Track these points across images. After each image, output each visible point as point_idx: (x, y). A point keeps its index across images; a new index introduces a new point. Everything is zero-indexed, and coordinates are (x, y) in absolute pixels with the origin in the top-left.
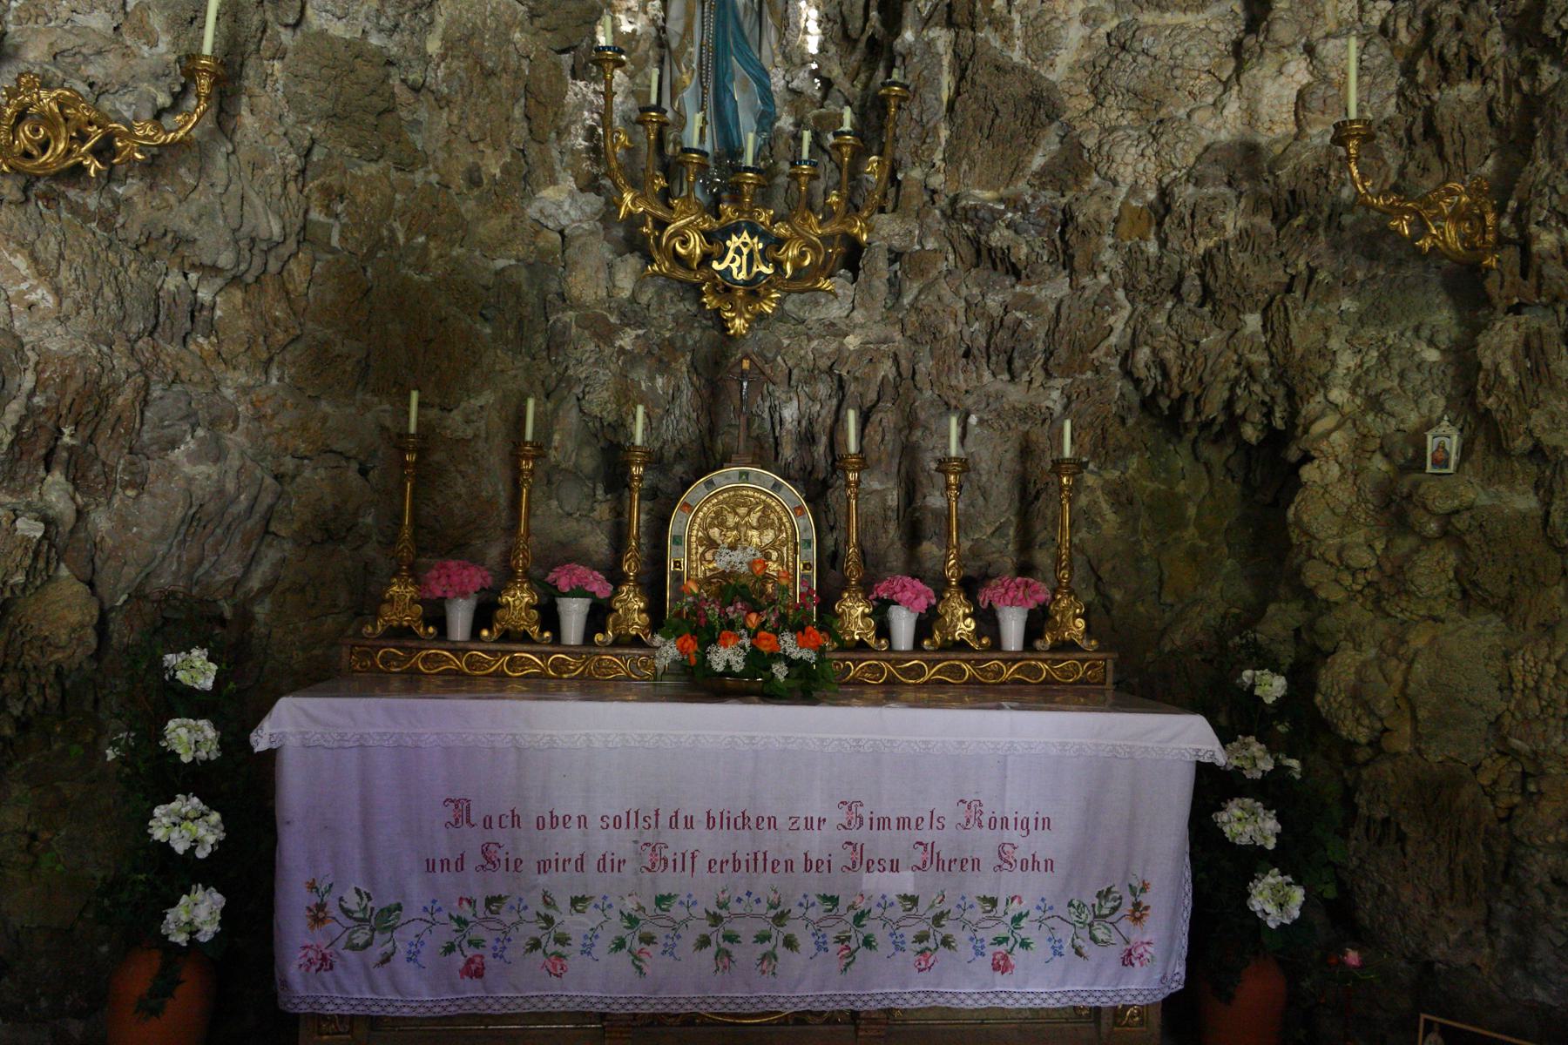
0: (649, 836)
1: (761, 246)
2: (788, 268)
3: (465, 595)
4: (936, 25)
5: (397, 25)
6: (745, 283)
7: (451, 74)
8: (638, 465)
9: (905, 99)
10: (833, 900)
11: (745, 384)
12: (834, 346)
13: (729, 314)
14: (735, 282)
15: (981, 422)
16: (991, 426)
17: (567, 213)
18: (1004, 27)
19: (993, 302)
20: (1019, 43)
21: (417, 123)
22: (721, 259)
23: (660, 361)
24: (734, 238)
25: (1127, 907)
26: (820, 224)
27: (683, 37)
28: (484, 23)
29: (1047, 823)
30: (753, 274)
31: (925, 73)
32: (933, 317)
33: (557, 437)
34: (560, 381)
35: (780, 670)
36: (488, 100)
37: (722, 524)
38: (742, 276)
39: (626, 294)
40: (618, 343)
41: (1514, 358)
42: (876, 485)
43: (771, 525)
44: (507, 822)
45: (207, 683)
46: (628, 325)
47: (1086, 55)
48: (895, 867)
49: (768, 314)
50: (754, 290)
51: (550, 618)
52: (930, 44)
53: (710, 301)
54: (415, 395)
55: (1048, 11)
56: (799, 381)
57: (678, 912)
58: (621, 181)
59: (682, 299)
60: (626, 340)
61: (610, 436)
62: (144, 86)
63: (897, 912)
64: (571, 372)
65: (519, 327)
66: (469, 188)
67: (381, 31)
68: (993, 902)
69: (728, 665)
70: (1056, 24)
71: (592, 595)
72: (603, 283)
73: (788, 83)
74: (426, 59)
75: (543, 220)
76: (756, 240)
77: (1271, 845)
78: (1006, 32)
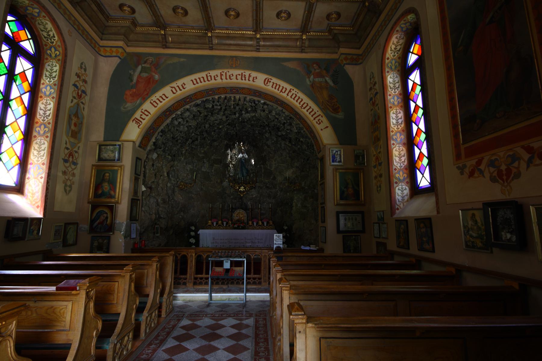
19: (268, 192)
35: (240, 227)
45: (194, 229)
50: (243, 192)
51: (223, 224)
53: (239, 193)
60: (232, 197)
74: (212, 172)
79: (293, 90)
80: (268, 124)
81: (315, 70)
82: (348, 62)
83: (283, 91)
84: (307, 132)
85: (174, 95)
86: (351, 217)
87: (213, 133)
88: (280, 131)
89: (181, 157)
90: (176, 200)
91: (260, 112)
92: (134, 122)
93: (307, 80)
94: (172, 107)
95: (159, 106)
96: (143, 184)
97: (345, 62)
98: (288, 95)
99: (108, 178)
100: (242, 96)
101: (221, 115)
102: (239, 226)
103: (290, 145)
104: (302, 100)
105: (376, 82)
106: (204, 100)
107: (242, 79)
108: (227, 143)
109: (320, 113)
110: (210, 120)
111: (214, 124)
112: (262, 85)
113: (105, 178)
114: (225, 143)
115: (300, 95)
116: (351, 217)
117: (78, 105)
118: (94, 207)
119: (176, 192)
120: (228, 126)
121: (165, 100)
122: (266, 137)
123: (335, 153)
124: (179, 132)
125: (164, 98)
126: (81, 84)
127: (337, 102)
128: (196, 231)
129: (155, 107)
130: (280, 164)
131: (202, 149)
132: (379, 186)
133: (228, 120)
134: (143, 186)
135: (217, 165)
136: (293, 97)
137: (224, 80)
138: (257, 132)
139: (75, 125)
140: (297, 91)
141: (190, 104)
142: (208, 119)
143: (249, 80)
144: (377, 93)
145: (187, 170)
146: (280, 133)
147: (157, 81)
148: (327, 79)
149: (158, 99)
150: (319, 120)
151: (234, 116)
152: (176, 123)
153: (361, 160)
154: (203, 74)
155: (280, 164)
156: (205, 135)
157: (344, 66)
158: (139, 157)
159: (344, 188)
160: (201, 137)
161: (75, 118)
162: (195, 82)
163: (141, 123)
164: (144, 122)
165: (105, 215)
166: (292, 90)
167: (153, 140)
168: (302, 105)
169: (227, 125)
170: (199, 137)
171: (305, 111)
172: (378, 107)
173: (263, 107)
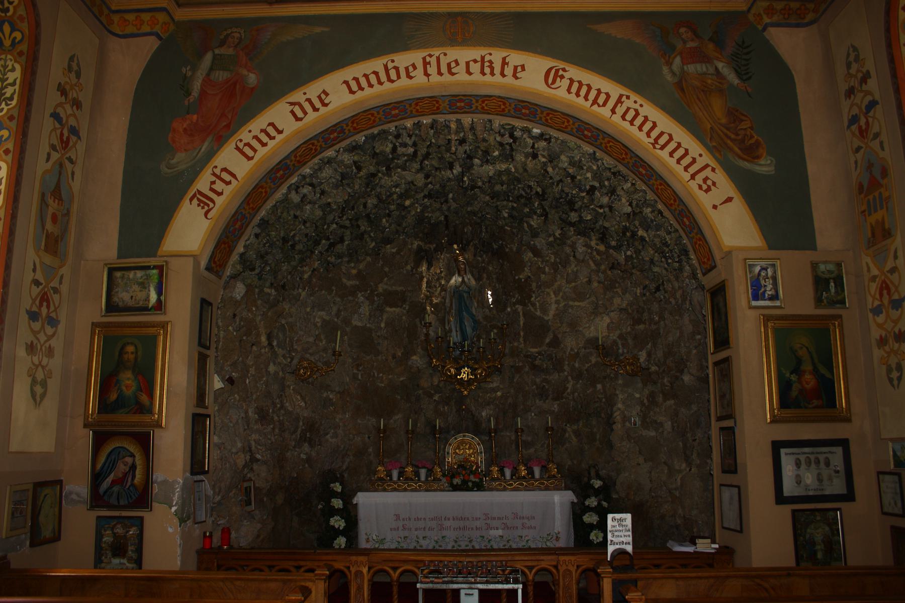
0: (440, 522)
3: (396, 469)
10: (483, 537)
15: (535, 415)
21: (379, 343)
22: (460, 375)
25: (555, 538)
29: (534, 518)
33: (419, 425)
35: (470, 484)
37: (459, 448)
39: (436, 383)
41: (647, 398)
42: (508, 434)
43: (472, 448)
44: (408, 519)
45: (339, 490)
47: (557, 312)
48: (497, 529)
51: (417, 474)
53: (458, 387)
57: (447, 540)
60: (436, 398)
62: (321, 353)
63: (498, 539)
68: (522, 537)
69: (457, 483)
70: (548, 305)
71: (427, 468)
77: (595, 523)
79: (628, 97)
80: (543, 191)
81: (685, 42)
82: (775, 18)
83: (601, 101)
84: (666, 213)
85: (299, 124)
86: (812, 457)
87: (384, 220)
88: (576, 211)
89: (300, 290)
90: (290, 409)
91: (523, 160)
92: (195, 201)
93: (665, 70)
94: (293, 158)
95: (258, 157)
96: (217, 372)
97: (767, 20)
98: (613, 111)
99: (132, 357)
100: (479, 118)
101: (413, 170)
102: (465, 482)
103: (602, 248)
104: (655, 125)
105: (868, 72)
106: (376, 132)
107: (483, 74)
108: (419, 247)
109: (707, 159)
110: (381, 187)
111: (392, 194)
112: (541, 87)
113: (126, 356)
114: (415, 246)
115: (649, 110)
116: (812, 457)
117: (61, 165)
118: (100, 440)
119: (289, 387)
120: (426, 200)
121: (274, 138)
122: (530, 226)
123: (759, 274)
124: (300, 222)
125: (273, 132)
126: (69, 112)
127: (752, 128)
128: (347, 496)
129: (250, 158)
130: (571, 303)
131: (352, 265)
132: (894, 366)
133: (431, 183)
134: (216, 378)
135: (394, 309)
136: (629, 117)
137: (435, 78)
138: (506, 215)
139: (54, 219)
140: (640, 101)
141: (337, 147)
142: (377, 184)
143: (503, 75)
144: (872, 104)
145: (315, 325)
146: (574, 217)
147: (253, 89)
148: (720, 65)
149: (256, 137)
150: (705, 180)
151: (448, 174)
152: (295, 198)
153: (833, 290)
154: (377, 64)
155: (571, 303)
156: (364, 226)
157: (764, 29)
158: (205, 297)
159: (791, 373)
160: (352, 233)
161: (54, 201)
162: (354, 87)
163: (211, 205)
164: (219, 200)
165: (129, 460)
166: (624, 98)
167: (240, 249)
168: (656, 140)
169: (425, 197)
170: (348, 232)
171: (664, 154)
172: (881, 143)
173: (533, 147)
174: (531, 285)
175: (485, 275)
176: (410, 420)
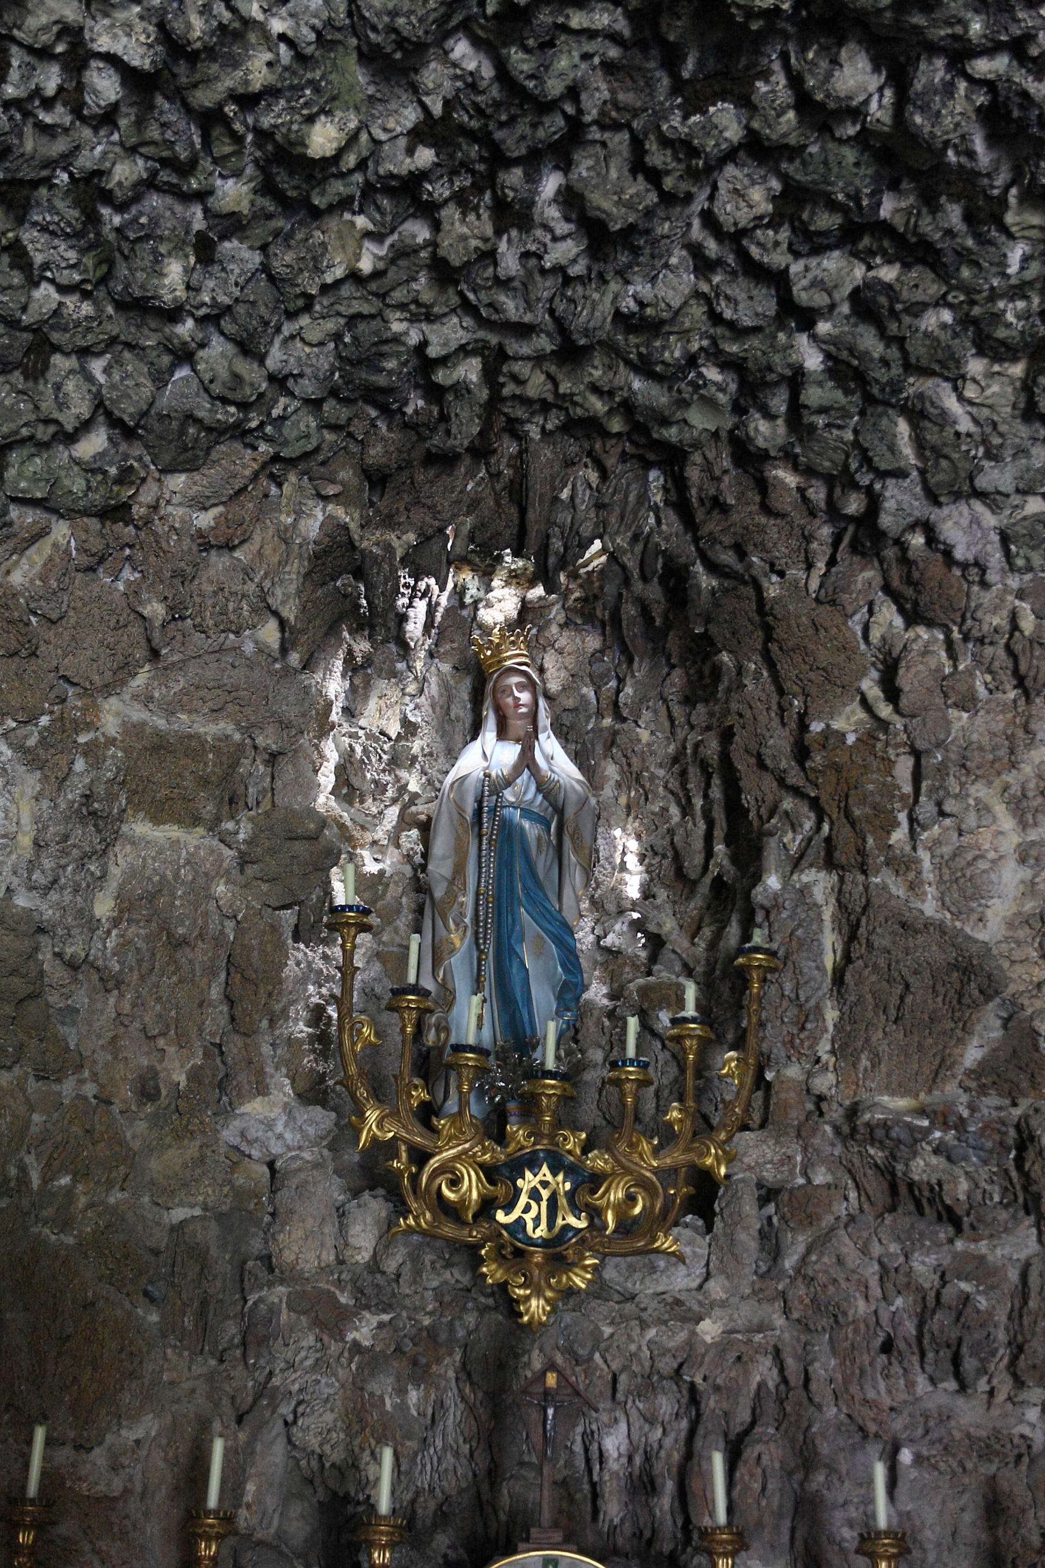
1: (568, 1186)
2: (610, 1217)
4: (811, 865)
5: (55, 881)
6: (545, 1243)
7: (125, 944)
8: (383, 1548)
9: (773, 970)
11: (550, 1412)
12: (682, 1336)
13: (520, 1292)
14: (531, 1242)
16: (935, 1467)
17: (280, 1137)
18: (908, 868)
20: (931, 891)
22: (509, 1208)
23: (415, 1363)
24: (528, 1175)
26: (656, 1151)
27: (451, 883)
28: (177, 875)
30: (557, 1230)
31: (799, 932)
32: (831, 1289)
33: (251, 1487)
34: (258, 1397)
36: (175, 978)
38: (541, 1232)
39: (364, 1257)
40: (350, 1336)
46: (368, 1307)
49: (580, 1289)
52: (804, 891)
53: (492, 1272)
54: (40, 1434)
55: (970, 847)
56: (628, 1393)
58: (362, 1092)
59: (448, 1265)
61: (332, 1484)
64: (276, 1381)
65: (202, 1312)
66: (141, 1104)
67: (31, 888)
70: (982, 865)
72: (330, 1242)
73: (599, 938)
74: (92, 924)
75: (244, 1147)
76: (560, 1177)
78: (911, 875)
87: (174, 271)
108: (337, 532)
114: (312, 526)
135: (172, 831)
174: (889, 765)
175: (611, 771)
176: (218, 1448)
